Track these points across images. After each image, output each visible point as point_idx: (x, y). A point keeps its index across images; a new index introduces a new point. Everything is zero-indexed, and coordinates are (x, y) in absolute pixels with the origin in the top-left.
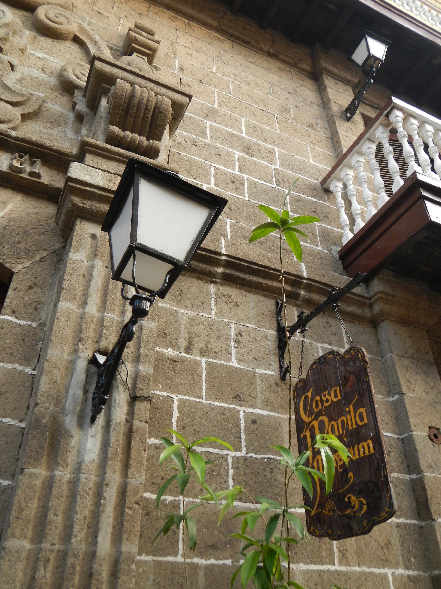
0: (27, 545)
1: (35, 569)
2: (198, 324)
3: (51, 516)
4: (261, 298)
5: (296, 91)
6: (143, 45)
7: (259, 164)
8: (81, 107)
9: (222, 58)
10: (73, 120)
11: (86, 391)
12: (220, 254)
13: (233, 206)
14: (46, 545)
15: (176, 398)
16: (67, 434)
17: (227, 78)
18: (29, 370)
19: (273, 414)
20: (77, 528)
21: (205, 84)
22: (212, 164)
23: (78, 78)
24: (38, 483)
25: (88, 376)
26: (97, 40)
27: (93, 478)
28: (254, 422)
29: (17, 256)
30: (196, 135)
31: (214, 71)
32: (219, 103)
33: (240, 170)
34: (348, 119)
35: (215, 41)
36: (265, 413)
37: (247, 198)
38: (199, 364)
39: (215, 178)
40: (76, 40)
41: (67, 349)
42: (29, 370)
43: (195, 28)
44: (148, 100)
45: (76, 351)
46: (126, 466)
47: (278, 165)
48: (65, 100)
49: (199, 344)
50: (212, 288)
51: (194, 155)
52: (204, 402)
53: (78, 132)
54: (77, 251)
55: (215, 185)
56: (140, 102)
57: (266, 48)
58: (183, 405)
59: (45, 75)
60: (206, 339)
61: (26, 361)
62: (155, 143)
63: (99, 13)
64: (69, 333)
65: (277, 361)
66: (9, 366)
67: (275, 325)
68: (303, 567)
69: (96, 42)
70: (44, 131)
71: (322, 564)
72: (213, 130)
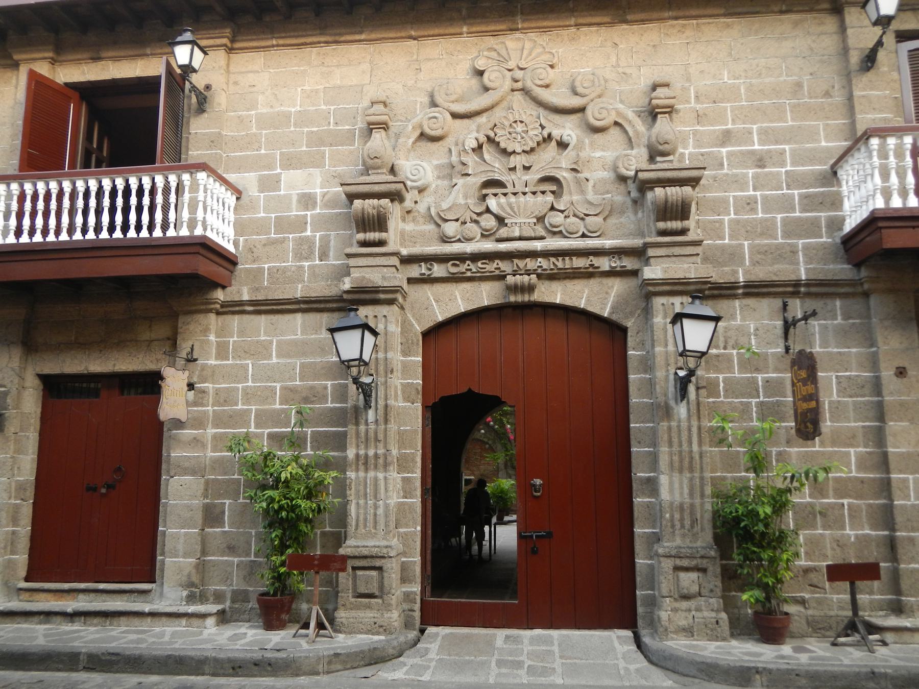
0: (667, 449)
1: (672, 456)
2: (729, 330)
3: (673, 439)
4: (771, 300)
5: (811, 49)
6: (663, 107)
7: (771, 173)
8: (634, 194)
9: (733, 52)
10: (631, 203)
11: (676, 388)
12: (739, 283)
13: (749, 228)
14: (674, 449)
15: (721, 376)
16: (672, 409)
17: (738, 81)
18: (648, 376)
19: (780, 375)
20: (683, 443)
21: (719, 102)
22: (731, 194)
23: (627, 170)
24: (665, 428)
25: (675, 380)
26: (630, 119)
27: (686, 424)
28: (767, 381)
29: (627, 318)
30: (716, 170)
31: (726, 80)
32: (733, 120)
33: (755, 190)
34: (868, 69)
35: (725, 32)
36: (774, 375)
37: (760, 215)
38: (732, 354)
39: (734, 207)
40: (616, 123)
41: (663, 371)
42: (648, 376)
43: (703, 27)
44: (677, 200)
45: (668, 371)
46: (699, 418)
47: (789, 165)
48: (622, 188)
49: (731, 342)
50: (737, 303)
51: (716, 192)
52: (737, 375)
53: (636, 213)
54: (657, 317)
55: (735, 214)
56: (672, 204)
57: (776, 9)
58: (725, 379)
59: (606, 173)
60: (735, 338)
61: (645, 372)
62: (686, 223)
63: (624, 73)
64: (663, 363)
65: (783, 341)
66: (639, 376)
67: (782, 318)
68: (796, 449)
69: (630, 121)
70: (617, 221)
71: (808, 447)
72: (730, 154)
